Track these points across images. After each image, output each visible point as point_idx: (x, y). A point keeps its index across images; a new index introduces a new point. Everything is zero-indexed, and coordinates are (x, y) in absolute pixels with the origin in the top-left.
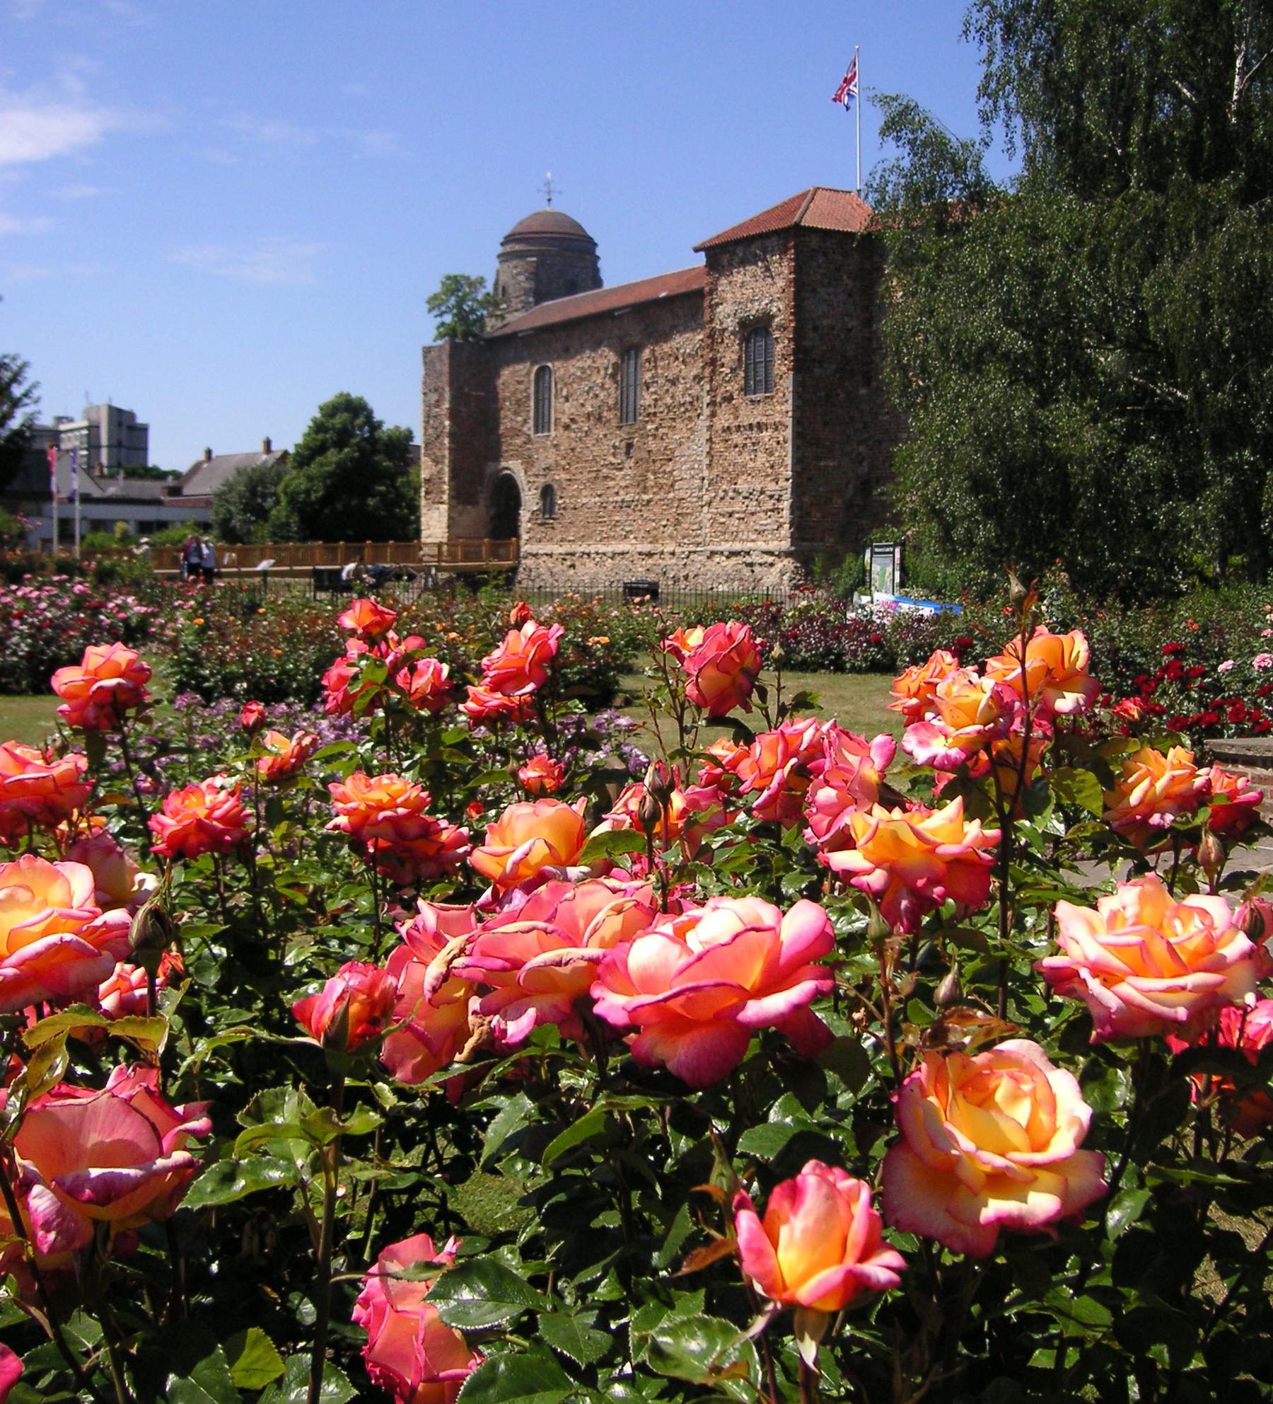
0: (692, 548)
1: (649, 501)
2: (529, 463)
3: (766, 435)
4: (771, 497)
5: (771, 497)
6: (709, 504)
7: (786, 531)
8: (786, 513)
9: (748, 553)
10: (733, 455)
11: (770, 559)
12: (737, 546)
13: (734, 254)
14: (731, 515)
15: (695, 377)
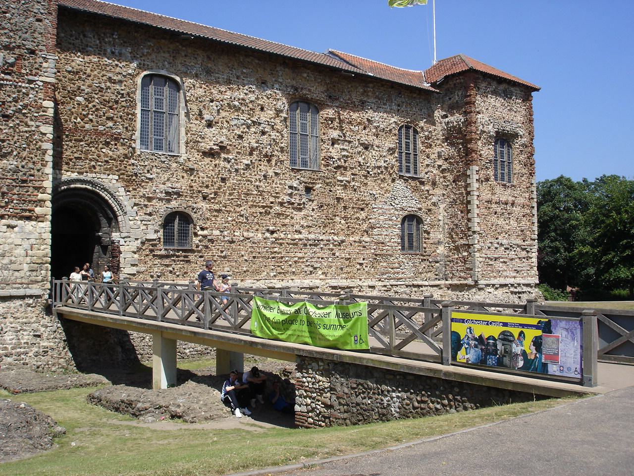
0: (393, 282)
1: (343, 241)
2: (131, 181)
3: (516, 209)
4: (525, 249)
5: (523, 249)
6: (479, 250)
7: (535, 271)
8: (535, 260)
9: (512, 285)
10: (493, 219)
11: (529, 289)
12: (502, 281)
13: (489, 84)
14: (496, 259)
15: (390, 149)
